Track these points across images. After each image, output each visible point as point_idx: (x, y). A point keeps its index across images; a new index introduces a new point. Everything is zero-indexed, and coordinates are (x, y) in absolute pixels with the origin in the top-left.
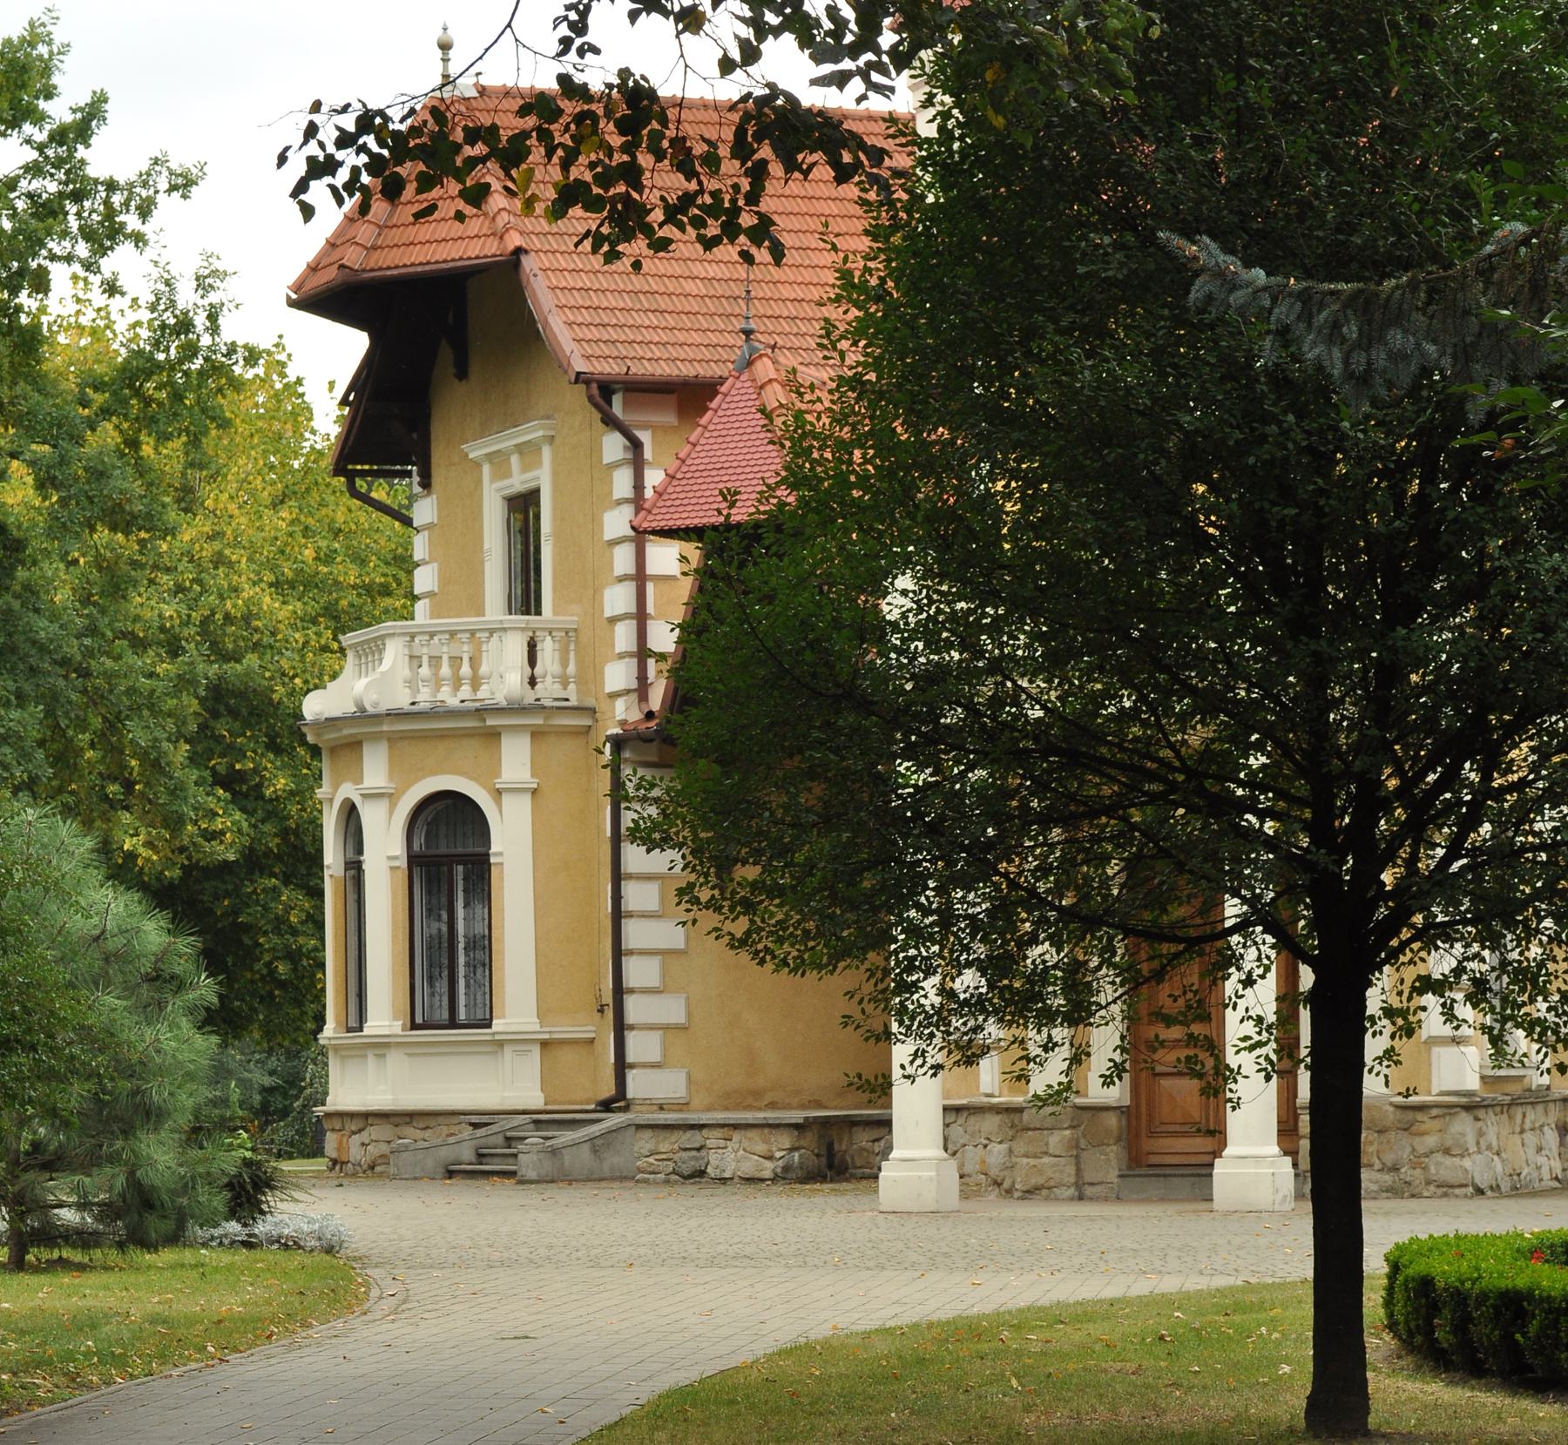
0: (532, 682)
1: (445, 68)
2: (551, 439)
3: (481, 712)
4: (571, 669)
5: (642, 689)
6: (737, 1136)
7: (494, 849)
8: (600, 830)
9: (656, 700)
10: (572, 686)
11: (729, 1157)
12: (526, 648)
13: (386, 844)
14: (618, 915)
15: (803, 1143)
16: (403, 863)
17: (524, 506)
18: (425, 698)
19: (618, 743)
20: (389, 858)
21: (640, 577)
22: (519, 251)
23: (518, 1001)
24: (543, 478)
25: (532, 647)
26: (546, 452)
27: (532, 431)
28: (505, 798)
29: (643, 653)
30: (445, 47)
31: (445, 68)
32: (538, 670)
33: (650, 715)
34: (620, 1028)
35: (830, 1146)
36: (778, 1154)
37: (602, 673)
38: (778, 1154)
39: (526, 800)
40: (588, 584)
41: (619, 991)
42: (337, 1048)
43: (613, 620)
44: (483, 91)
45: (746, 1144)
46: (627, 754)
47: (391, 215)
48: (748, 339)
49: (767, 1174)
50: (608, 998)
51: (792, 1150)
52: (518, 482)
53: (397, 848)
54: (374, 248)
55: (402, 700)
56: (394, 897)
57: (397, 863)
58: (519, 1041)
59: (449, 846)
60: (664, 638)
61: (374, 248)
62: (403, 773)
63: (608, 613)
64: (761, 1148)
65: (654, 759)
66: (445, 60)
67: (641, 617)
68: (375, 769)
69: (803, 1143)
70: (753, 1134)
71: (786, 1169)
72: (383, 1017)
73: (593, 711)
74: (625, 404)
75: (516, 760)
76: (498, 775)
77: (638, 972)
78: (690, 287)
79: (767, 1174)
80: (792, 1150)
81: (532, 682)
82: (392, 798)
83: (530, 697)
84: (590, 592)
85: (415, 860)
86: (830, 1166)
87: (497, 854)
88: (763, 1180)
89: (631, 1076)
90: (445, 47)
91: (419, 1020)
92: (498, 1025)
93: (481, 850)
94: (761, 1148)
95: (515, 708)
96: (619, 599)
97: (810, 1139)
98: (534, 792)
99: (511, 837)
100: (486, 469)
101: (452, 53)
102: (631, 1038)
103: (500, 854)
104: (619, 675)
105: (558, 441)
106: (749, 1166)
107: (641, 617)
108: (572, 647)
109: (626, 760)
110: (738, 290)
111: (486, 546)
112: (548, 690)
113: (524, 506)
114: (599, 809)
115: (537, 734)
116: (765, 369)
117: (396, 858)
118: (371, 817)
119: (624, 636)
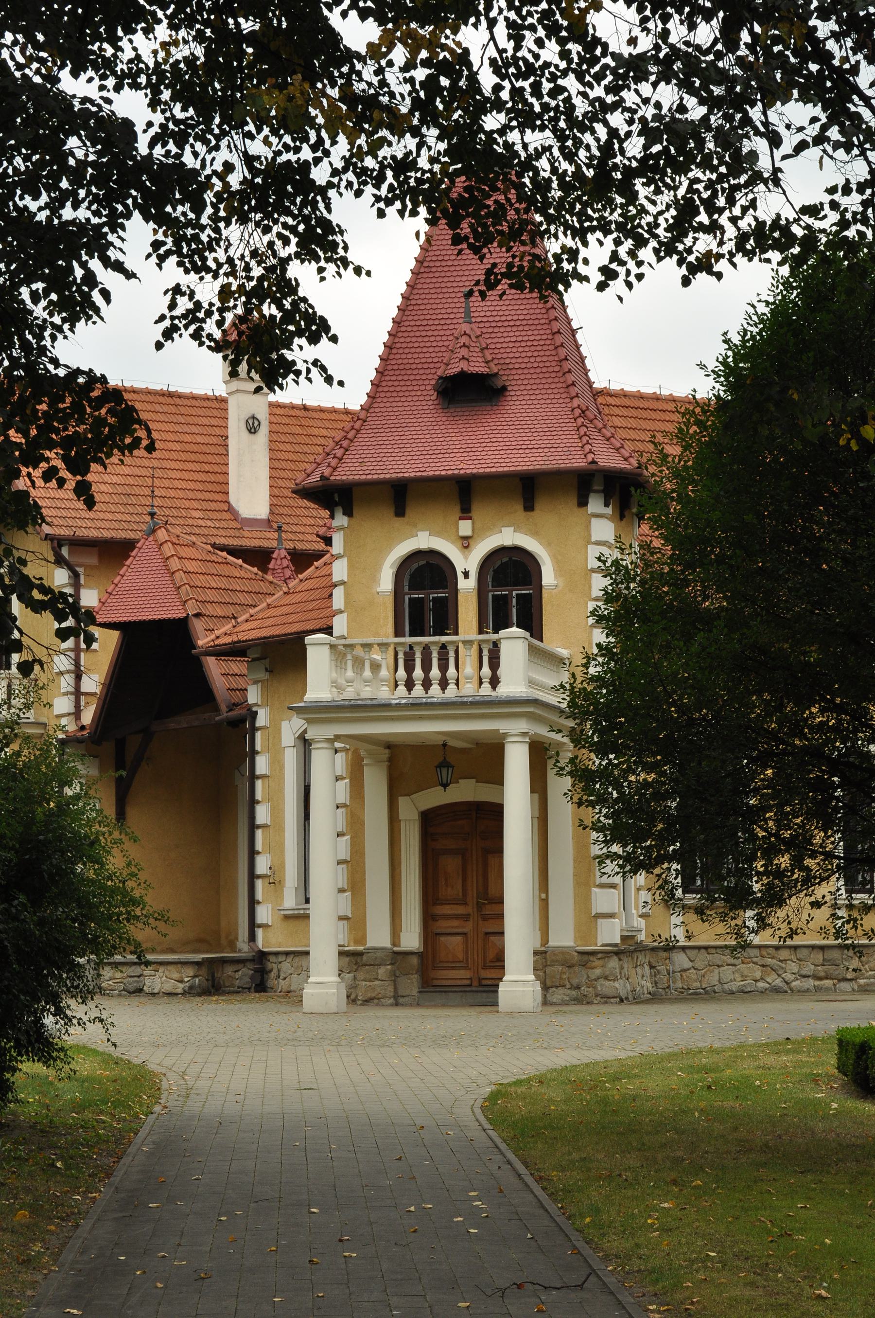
6: (161, 969)
15: (200, 973)
36: (186, 979)
38: (186, 979)
45: (167, 973)
49: (180, 991)
64: (176, 975)
69: (200, 973)
71: (191, 988)
79: (180, 991)
86: (213, 986)
88: (177, 994)
94: (176, 975)
97: (204, 971)
106: (169, 986)
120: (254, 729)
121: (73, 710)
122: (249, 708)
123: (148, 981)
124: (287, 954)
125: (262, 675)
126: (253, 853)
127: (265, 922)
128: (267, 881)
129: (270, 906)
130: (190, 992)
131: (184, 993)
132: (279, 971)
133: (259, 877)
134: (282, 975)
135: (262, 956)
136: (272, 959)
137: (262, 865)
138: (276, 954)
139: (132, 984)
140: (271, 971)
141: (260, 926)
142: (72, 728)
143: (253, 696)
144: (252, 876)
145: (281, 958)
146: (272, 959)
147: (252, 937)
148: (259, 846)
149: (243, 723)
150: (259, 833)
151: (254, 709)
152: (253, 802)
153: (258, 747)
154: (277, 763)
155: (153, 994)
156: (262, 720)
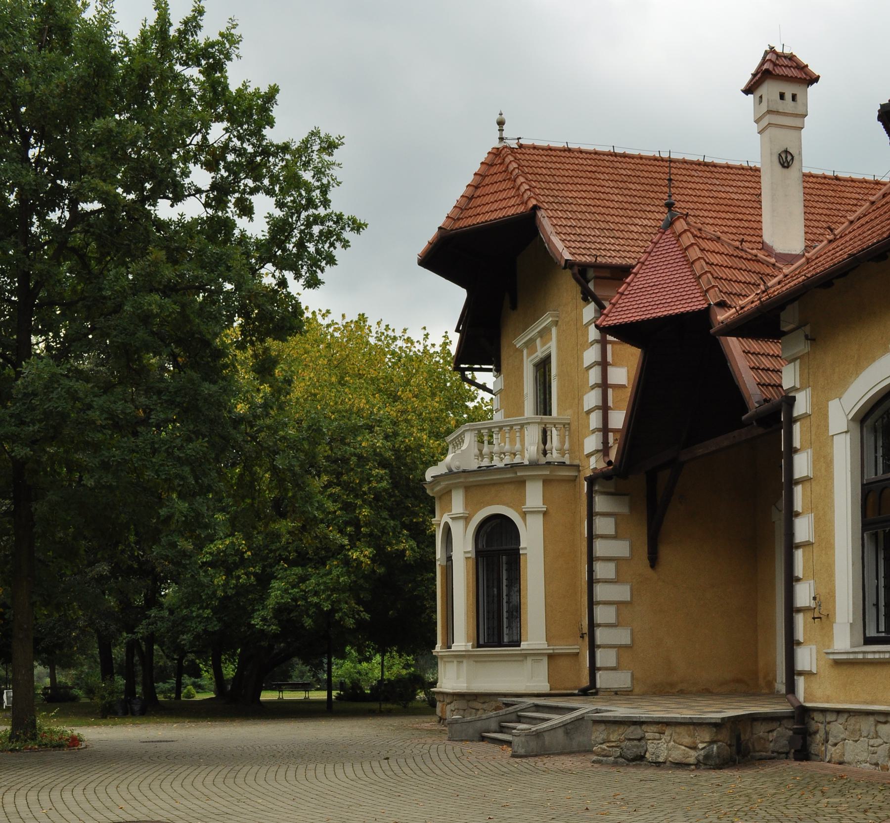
0: (545, 453)
1: (501, 134)
2: (556, 323)
3: (513, 467)
4: (567, 446)
5: (605, 449)
6: (668, 732)
7: (522, 546)
8: (581, 534)
9: (613, 456)
10: (567, 455)
11: (662, 747)
12: (541, 434)
13: (463, 545)
14: (591, 582)
15: (720, 737)
16: (473, 555)
17: (543, 366)
18: (486, 462)
19: (591, 481)
20: (465, 552)
21: (604, 385)
22: (535, 208)
23: (535, 632)
24: (552, 347)
25: (545, 432)
26: (554, 330)
27: (546, 320)
28: (528, 517)
29: (605, 429)
30: (501, 123)
31: (501, 134)
32: (548, 446)
33: (610, 463)
34: (593, 647)
35: (738, 738)
36: (701, 746)
37: (583, 444)
38: (701, 746)
39: (540, 518)
40: (574, 396)
41: (592, 625)
42: (442, 657)
43: (589, 412)
44: (521, 146)
45: (675, 736)
46: (596, 488)
47: (468, 204)
48: (670, 210)
49: (692, 760)
50: (586, 630)
51: (712, 742)
52: (540, 354)
53: (470, 546)
54: (458, 219)
55: (474, 465)
56: (468, 572)
57: (469, 555)
58: (535, 655)
59: (498, 546)
60: (618, 419)
61: (458, 219)
62: (472, 504)
63: (586, 409)
64: (687, 740)
65: (612, 490)
66: (501, 130)
67: (605, 408)
68: (458, 504)
69: (720, 737)
70: (681, 730)
71: (707, 757)
72: (462, 642)
73: (578, 466)
74: (595, 286)
75: (534, 495)
76: (524, 504)
77: (603, 614)
78: (633, 228)
79: (692, 760)
80: (712, 742)
81: (545, 453)
83: (543, 460)
84: (576, 400)
85: (479, 553)
86: (739, 752)
87: (523, 549)
88: (689, 765)
89: (599, 675)
90: (501, 123)
91: (481, 642)
92: (524, 645)
93: (513, 547)
94: (687, 740)
95: (534, 465)
96: (592, 399)
97: (725, 735)
98: (545, 514)
99: (532, 538)
100: (525, 352)
101: (504, 127)
102: (599, 653)
103: (525, 548)
104: (592, 443)
105: (559, 323)
106: (677, 755)
107: (605, 408)
108: (567, 433)
109: (596, 491)
110: (667, 170)
111: (525, 392)
112: (554, 456)
113: (543, 366)
114: (581, 522)
115: (546, 482)
116: (680, 226)
117: (469, 552)
118: (457, 529)
119: (595, 421)
120: (791, 421)
121: (601, 447)
123: (651, 747)
124: (839, 712)
125: (803, 348)
126: (791, 580)
127: (807, 668)
128: (810, 615)
129: (814, 647)
130: (708, 763)
131: (698, 765)
132: (827, 733)
133: (799, 610)
134: (832, 740)
135: (803, 714)
136: (818, 717)
137: (803, 595)
138: (824, 711)
139: (632, 749)
140: (816, 732)
141: (801, 673)
142: (602, 465)
143: (789, 378)
144: (791, 610)
145: (829, 717)
146: (818, 717)
147: (791, 687)
148: (799, 571)
149: (778, 415)
150: (799, 555)
151: (792, 394)
152: (791, 515)
153: (797, 443)
154: (824, 461)
155: (658, 764)
156: (802, 406)
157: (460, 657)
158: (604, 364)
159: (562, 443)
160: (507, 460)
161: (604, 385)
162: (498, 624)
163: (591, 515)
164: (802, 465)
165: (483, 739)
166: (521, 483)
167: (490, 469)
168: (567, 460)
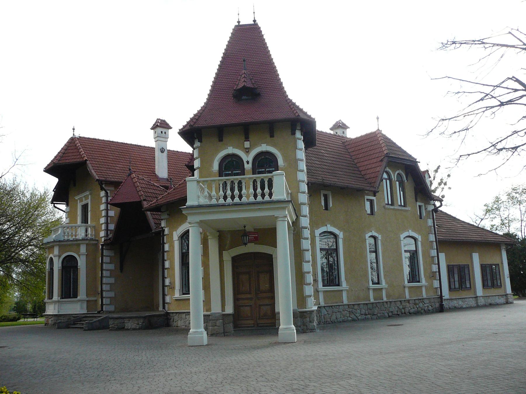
18: (66, 238)
82: (59, 256)
83: (86, 238)
95: (83, 240)
107: (107, 223)
120: (164, 235)
122: (162, 228)
126: (164, 278)
152: (164, 260)
153: (165, 242)
154: (172, 246)
157: (55, 302)
158: (107, 210)
159: (92, 232)
160: (74, 237)
161: (107, 216)
162: (69, 291)
163: (102, 256)
164: (167, 247)
165: (69, 328)
166: (79, 245)
167: (68, 240)
168: (93, 237)
